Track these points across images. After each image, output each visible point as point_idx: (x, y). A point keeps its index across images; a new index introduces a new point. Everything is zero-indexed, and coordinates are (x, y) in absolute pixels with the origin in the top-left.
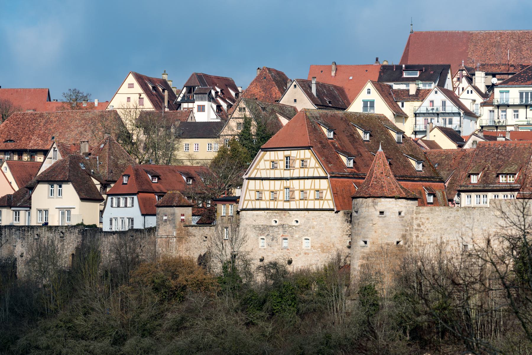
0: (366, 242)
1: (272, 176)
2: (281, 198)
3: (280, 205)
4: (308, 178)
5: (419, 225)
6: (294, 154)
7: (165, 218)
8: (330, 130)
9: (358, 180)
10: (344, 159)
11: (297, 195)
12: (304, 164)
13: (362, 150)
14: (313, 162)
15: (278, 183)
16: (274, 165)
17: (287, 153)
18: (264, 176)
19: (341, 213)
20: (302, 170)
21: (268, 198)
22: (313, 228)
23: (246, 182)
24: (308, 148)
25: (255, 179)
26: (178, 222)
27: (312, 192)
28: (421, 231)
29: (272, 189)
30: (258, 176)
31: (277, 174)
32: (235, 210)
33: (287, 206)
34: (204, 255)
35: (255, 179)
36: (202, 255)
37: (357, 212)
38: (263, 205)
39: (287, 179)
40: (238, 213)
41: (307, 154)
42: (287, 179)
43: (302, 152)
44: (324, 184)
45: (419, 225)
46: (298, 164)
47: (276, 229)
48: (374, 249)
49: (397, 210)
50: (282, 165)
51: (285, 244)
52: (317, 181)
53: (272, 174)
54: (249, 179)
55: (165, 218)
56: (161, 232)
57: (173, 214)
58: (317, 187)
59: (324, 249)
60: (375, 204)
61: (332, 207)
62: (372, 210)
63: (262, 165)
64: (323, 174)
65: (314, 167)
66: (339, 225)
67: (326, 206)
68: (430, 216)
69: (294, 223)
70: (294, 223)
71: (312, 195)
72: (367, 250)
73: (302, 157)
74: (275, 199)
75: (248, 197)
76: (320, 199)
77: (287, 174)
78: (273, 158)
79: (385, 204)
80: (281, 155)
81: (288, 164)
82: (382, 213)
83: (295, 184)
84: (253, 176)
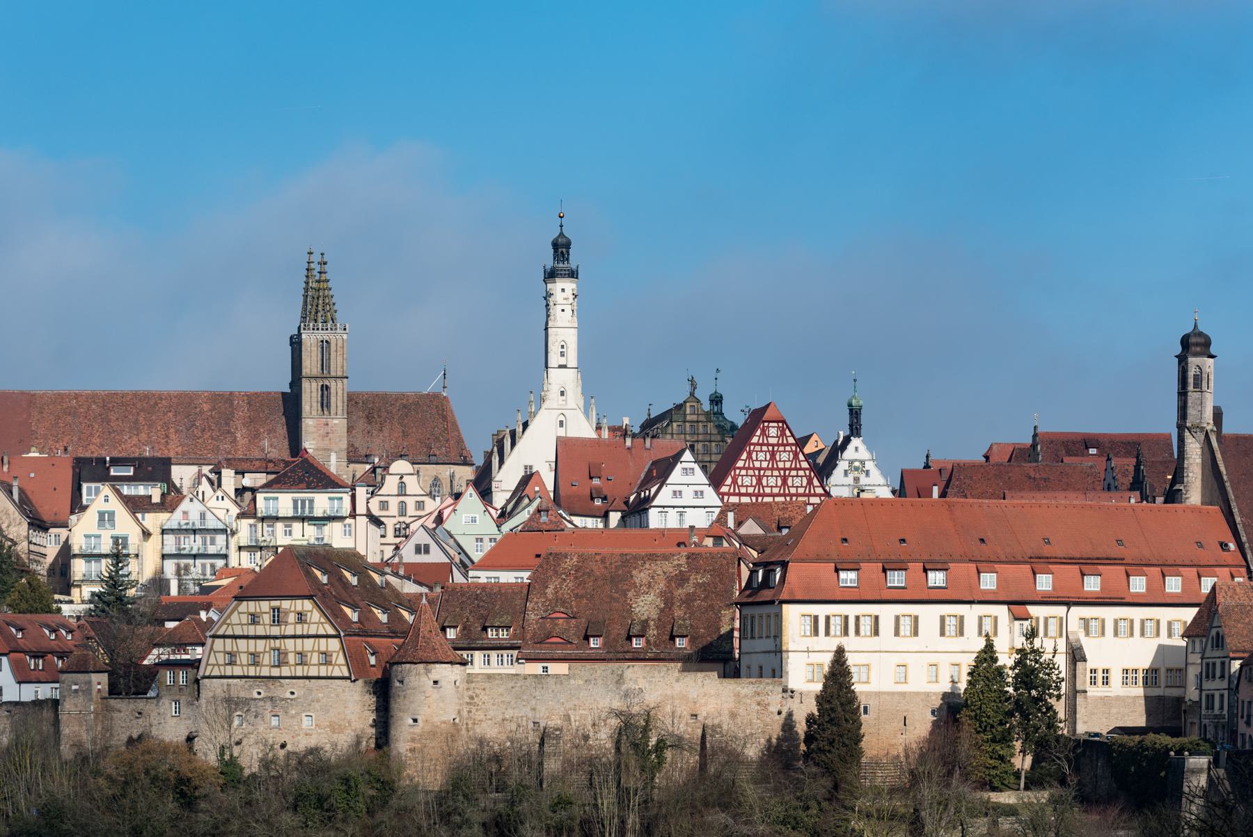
0: (415, 721)
1: (252, 633)
2: (266, 661)
3: (265, 672)
4: (309, 637)
5: (472, 698)
6: (286, 604)
7: (74, 687)
8: (324, 573)
9: (369, 639)
10: (348, 611)
11: (291, 658)
12: (301, 618)
13: (357, 598)
14: (316, 616)
15: (261, 643)
16: (254, 619)
17: (275, 603)
18: (238, 632)
19: (360, 682)
20: (299, 627)
21: (245, 662)
22: (318, 701)
23: (209, 641)
24: (310, 597)
25: (224, 637)
26: (94, 693)
27: (315, 655)
28: (475, 705)
29: (252, 649)
30: (229, 632)
31: (260, 631)
32: (191, 676)
33: (275, 672)
34: (140, 737)
35: (224, 637)
36: (135, 736)
37: (402, 682)
38: (238, 671)
39: (275, 638)
40: (197, 681)
41: (308, 605)
42: (275, 638)
43: (299, 602)
44: (334, 644)
45: (472, 698)
46: (292, 618)
47: (261, 703)
48: (428, 728)
49: (453, 678)
50: (267, 619)
51: (275, 721)
52: (323, 641)
53: (251, 630)
54: (215, 637)
55: (74, 687)
56: (68, 706)
57: (90, 683)
58: (323, 649)
59: (334, 728)
60: (428, 671)
61: (347, 674)
62: (424, 679)
63: (235, 618)
64: (331, 631)
65: (316, 621)
66: (357, 697)
67: (337, 673)
68: (487, 685)
69: (288, 695)
70: (288, 695)
71: (315, 659)
72: (417, 730)
73: (299, 609)
74: (256, 664)
75: (212, 660)
76: (328, 663)
77: (275, 631)
78: (252, 610)
79: (440, 671)
80: (265, 606)
81: (278, 617)
82: (436, 682)
83: (289, 644)
84: (220, 632)
